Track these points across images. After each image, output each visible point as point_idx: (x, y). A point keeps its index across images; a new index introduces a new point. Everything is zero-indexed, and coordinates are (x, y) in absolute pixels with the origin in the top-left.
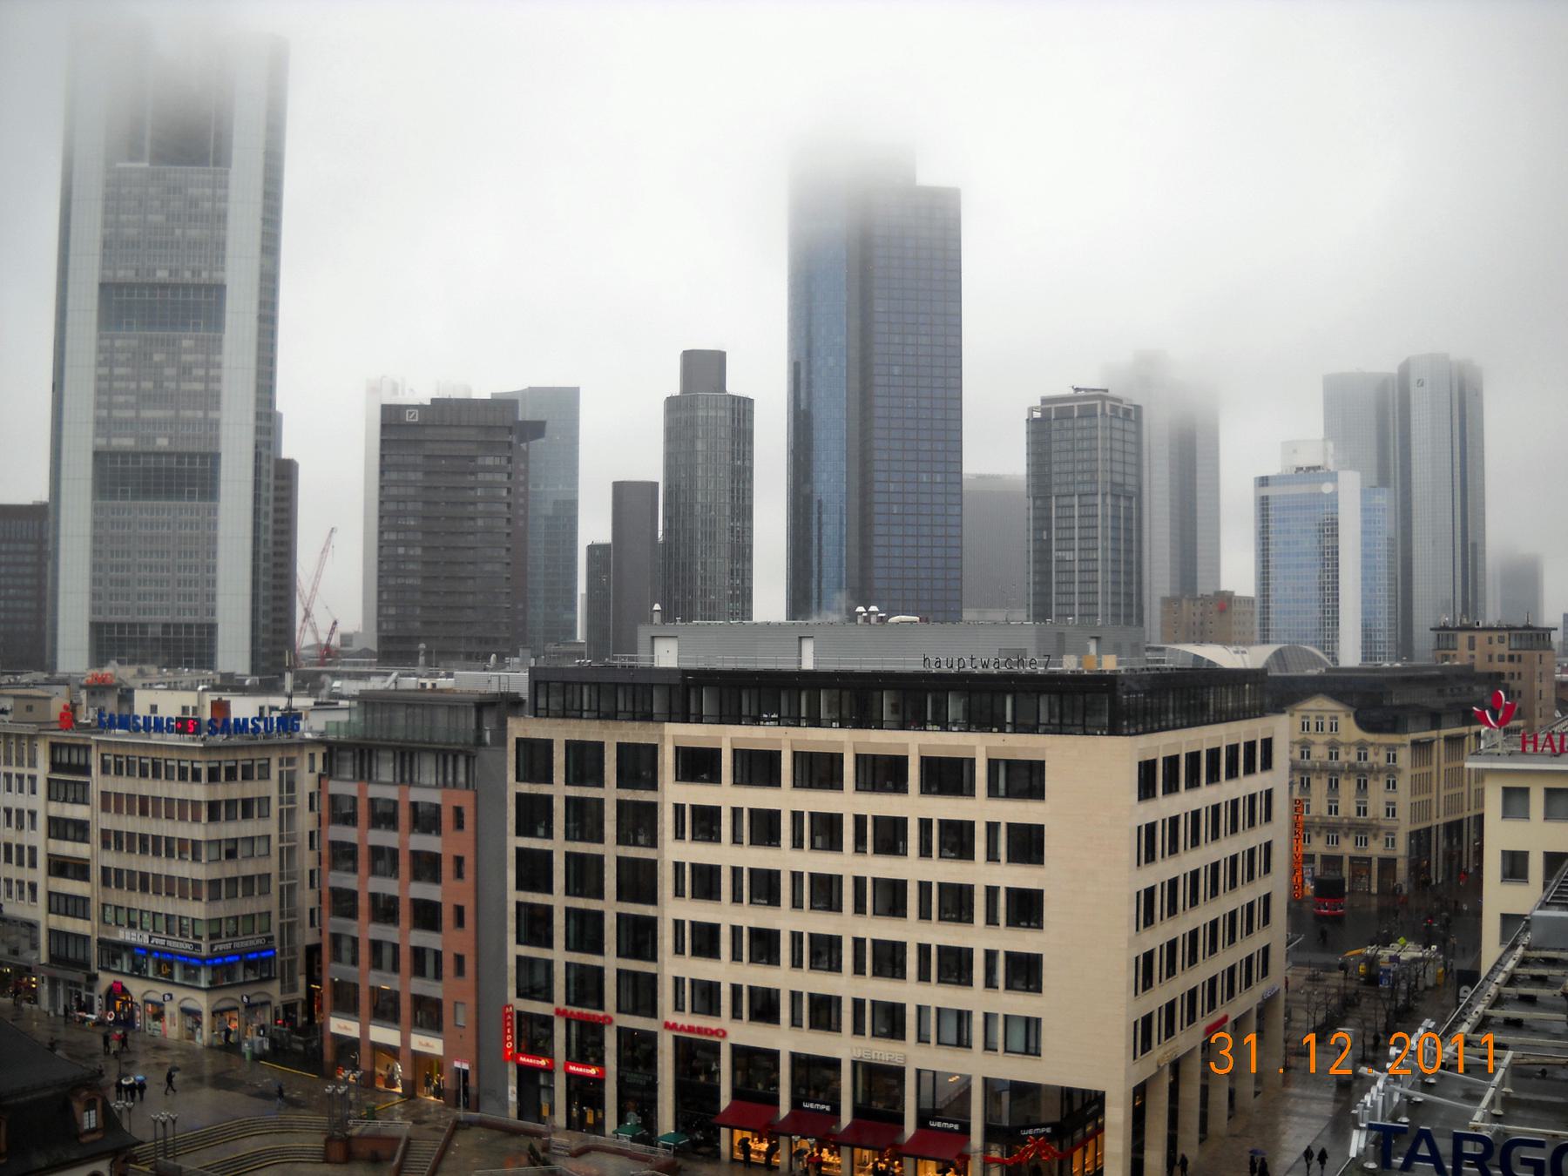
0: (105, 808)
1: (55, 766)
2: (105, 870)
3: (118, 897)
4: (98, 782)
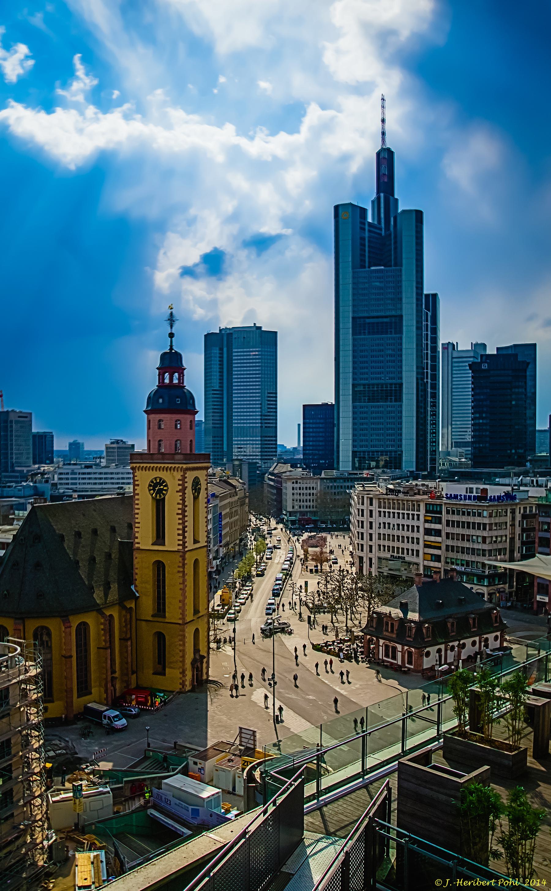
0: (448, 525)
1: (427, 511)
2: (447, 546)
3: (451, 555)
4: (445, 517)
